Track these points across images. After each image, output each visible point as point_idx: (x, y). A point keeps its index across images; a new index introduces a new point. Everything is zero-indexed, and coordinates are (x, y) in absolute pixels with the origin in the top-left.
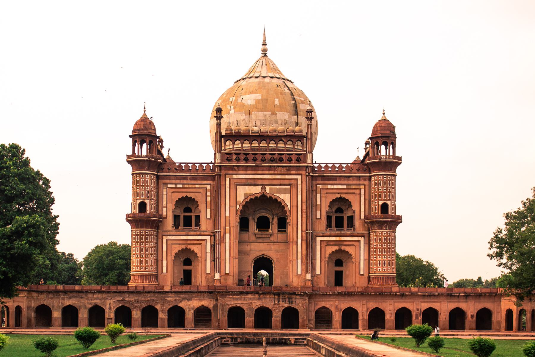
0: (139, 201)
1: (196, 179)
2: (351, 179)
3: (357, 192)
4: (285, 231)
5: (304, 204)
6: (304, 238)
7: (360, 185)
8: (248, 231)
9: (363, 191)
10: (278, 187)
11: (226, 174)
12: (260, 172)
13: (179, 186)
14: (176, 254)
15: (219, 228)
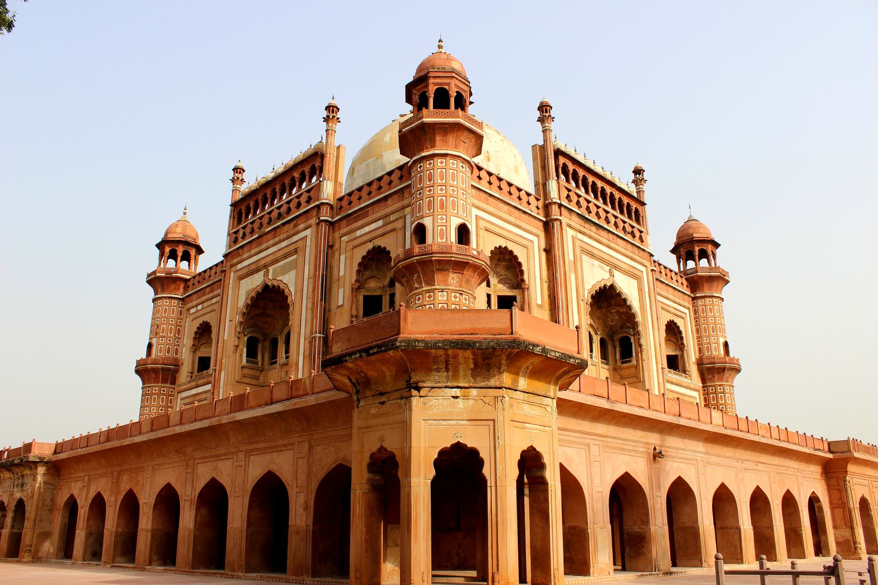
2: (389, 202)
3: (400, 224)
5: (311, 281)
6: (307, 353)
7: (403, 208)
10: (282, 263)
11: (232, 266)
12: (264, 246)
13: (200, 307)
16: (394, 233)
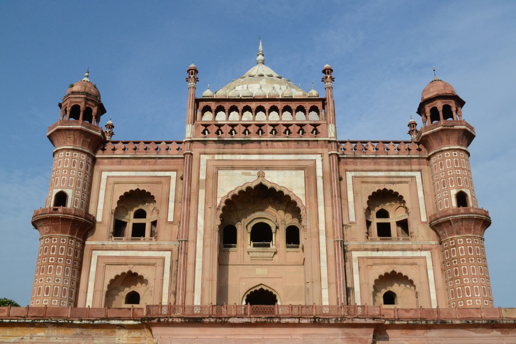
0: (56, 191)
1: (155, 164)
4: (298, 247)
8: (235, 247)
9: (419, 180)
14: (112, 281)
15: (187, 236)
16: (407, 185)
